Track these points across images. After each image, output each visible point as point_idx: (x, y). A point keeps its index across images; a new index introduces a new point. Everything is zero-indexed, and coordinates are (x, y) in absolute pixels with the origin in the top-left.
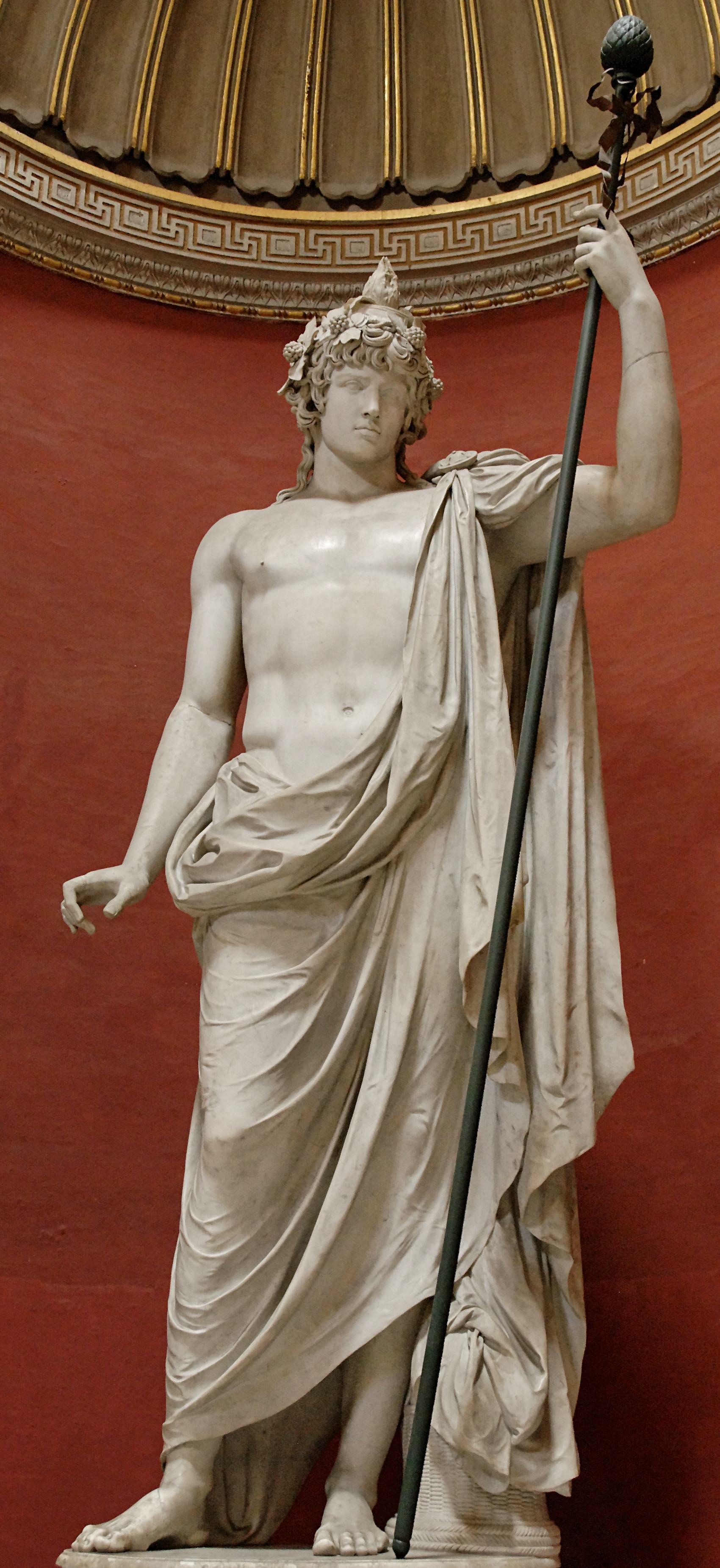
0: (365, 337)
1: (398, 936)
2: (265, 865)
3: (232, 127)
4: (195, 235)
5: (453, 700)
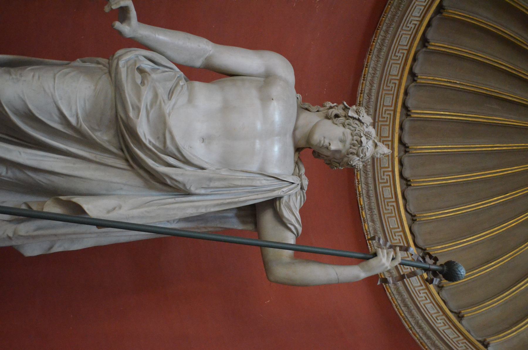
0: (361, 148)
1: (93, 166)
2: (133, 108)
3: (443, 50)
4: (405, 34)
5: (203, 191)
